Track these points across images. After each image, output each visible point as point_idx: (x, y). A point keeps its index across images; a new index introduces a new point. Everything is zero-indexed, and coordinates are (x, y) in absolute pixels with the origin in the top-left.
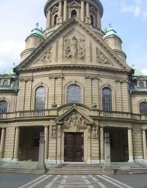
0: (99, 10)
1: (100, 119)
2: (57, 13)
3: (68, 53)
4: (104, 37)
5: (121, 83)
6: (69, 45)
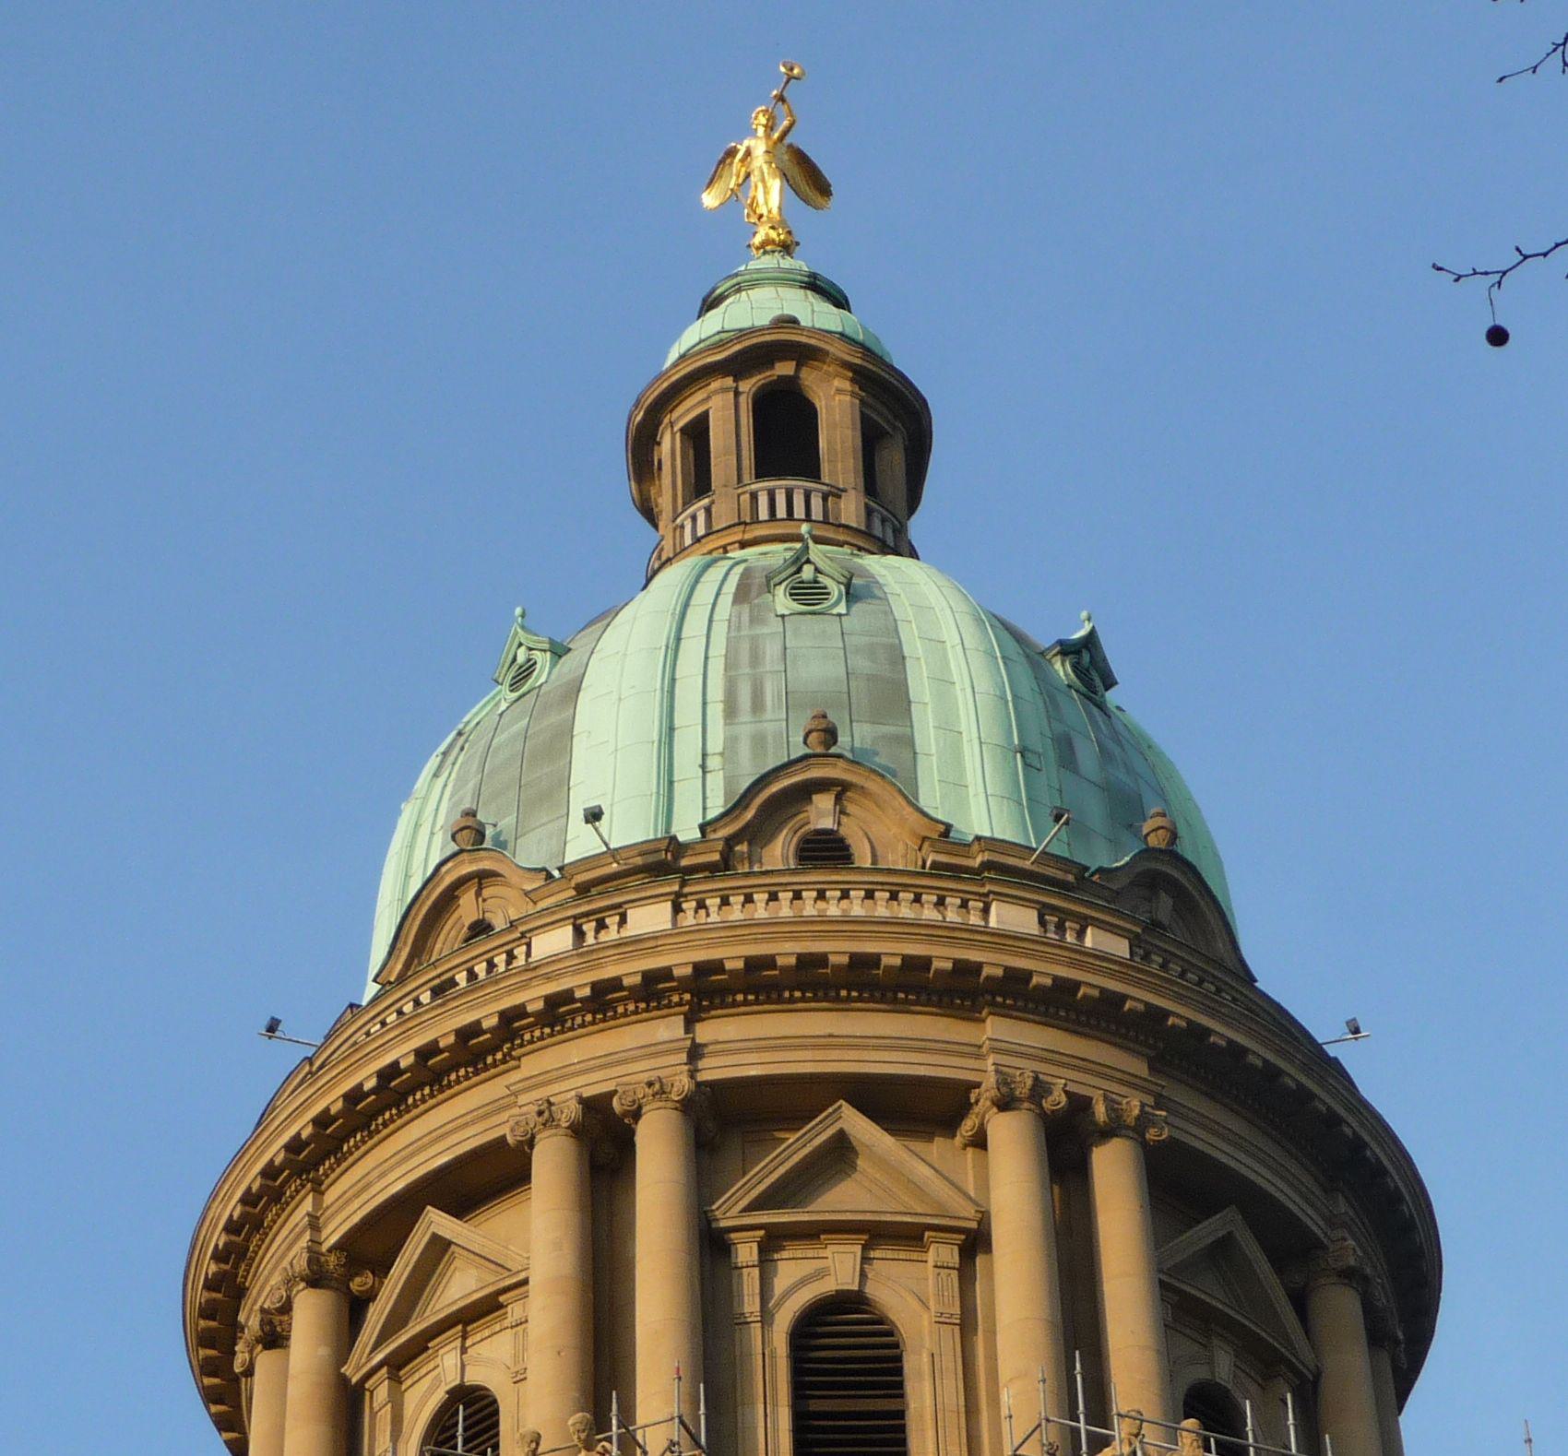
0: (1349, 1276)
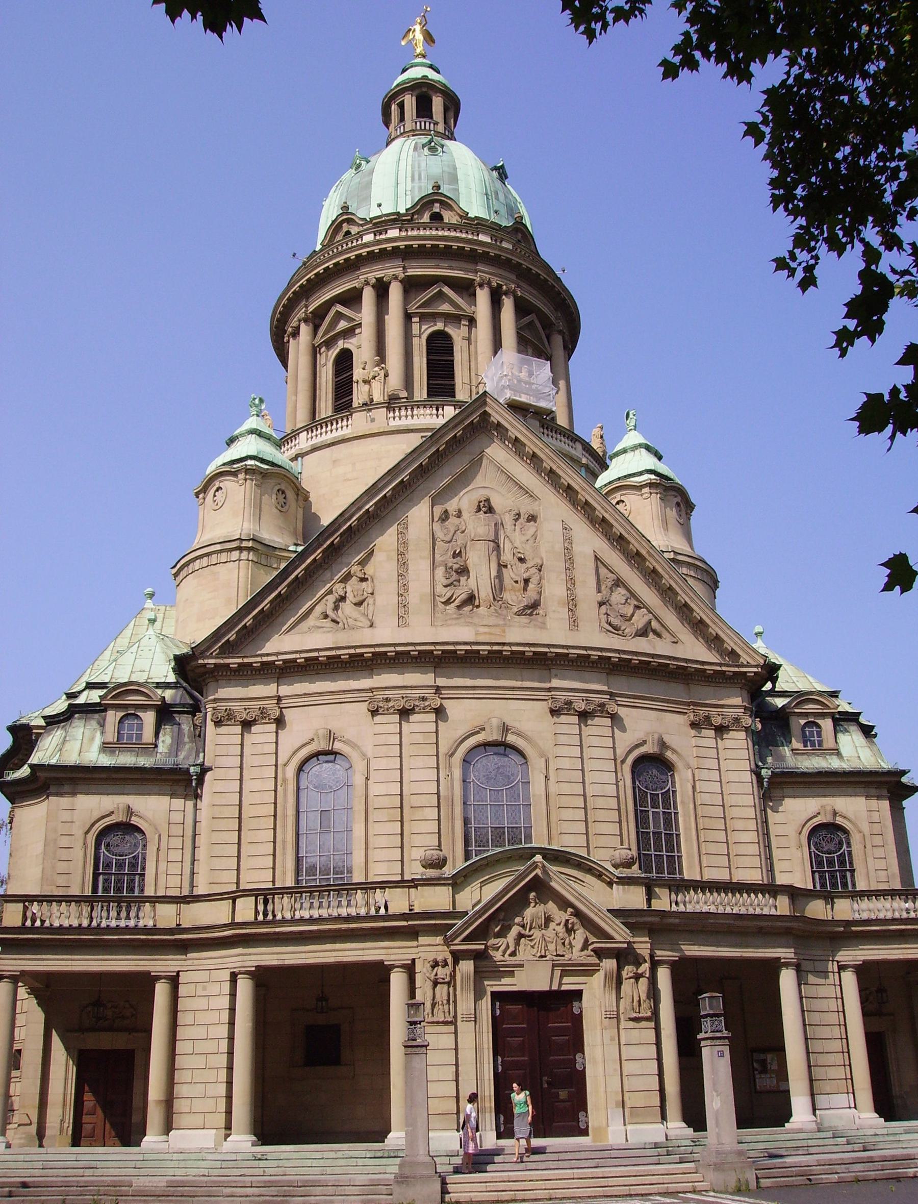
2: (350, 344)
3: (459, 581)
4: (603, 479)
5: (721, 730)
6: (460, 539)
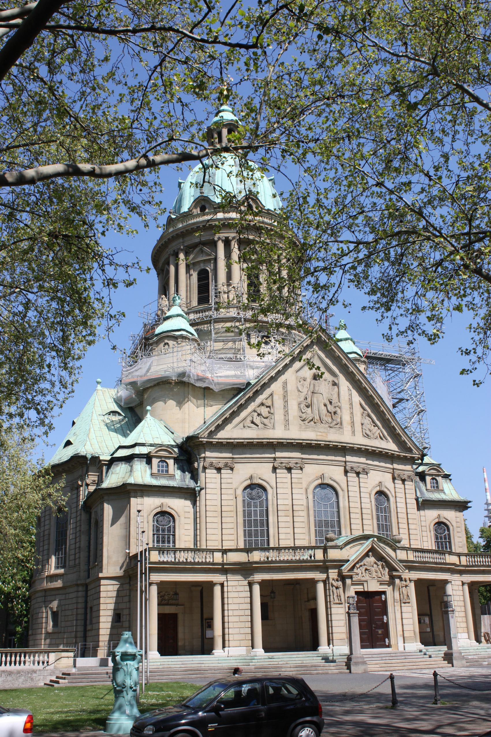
1: (410, 566)
